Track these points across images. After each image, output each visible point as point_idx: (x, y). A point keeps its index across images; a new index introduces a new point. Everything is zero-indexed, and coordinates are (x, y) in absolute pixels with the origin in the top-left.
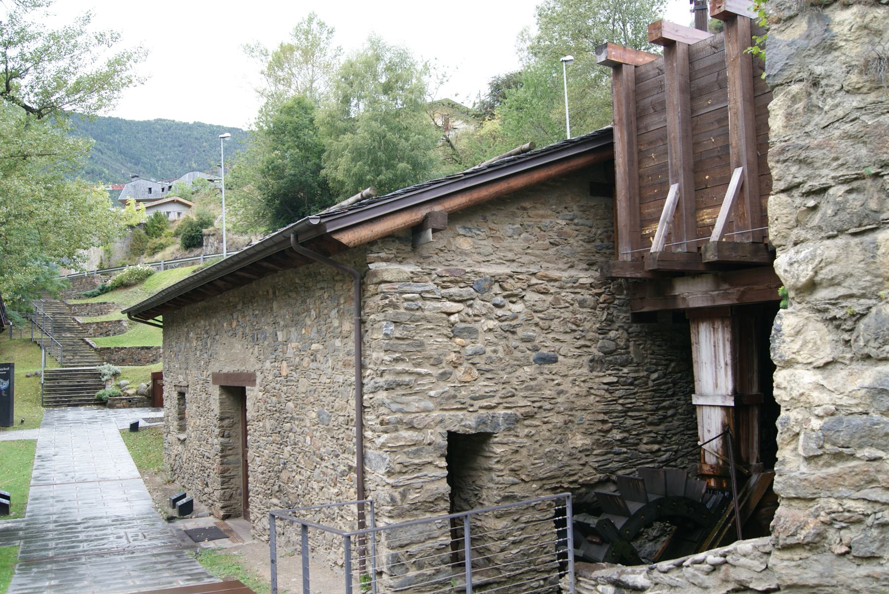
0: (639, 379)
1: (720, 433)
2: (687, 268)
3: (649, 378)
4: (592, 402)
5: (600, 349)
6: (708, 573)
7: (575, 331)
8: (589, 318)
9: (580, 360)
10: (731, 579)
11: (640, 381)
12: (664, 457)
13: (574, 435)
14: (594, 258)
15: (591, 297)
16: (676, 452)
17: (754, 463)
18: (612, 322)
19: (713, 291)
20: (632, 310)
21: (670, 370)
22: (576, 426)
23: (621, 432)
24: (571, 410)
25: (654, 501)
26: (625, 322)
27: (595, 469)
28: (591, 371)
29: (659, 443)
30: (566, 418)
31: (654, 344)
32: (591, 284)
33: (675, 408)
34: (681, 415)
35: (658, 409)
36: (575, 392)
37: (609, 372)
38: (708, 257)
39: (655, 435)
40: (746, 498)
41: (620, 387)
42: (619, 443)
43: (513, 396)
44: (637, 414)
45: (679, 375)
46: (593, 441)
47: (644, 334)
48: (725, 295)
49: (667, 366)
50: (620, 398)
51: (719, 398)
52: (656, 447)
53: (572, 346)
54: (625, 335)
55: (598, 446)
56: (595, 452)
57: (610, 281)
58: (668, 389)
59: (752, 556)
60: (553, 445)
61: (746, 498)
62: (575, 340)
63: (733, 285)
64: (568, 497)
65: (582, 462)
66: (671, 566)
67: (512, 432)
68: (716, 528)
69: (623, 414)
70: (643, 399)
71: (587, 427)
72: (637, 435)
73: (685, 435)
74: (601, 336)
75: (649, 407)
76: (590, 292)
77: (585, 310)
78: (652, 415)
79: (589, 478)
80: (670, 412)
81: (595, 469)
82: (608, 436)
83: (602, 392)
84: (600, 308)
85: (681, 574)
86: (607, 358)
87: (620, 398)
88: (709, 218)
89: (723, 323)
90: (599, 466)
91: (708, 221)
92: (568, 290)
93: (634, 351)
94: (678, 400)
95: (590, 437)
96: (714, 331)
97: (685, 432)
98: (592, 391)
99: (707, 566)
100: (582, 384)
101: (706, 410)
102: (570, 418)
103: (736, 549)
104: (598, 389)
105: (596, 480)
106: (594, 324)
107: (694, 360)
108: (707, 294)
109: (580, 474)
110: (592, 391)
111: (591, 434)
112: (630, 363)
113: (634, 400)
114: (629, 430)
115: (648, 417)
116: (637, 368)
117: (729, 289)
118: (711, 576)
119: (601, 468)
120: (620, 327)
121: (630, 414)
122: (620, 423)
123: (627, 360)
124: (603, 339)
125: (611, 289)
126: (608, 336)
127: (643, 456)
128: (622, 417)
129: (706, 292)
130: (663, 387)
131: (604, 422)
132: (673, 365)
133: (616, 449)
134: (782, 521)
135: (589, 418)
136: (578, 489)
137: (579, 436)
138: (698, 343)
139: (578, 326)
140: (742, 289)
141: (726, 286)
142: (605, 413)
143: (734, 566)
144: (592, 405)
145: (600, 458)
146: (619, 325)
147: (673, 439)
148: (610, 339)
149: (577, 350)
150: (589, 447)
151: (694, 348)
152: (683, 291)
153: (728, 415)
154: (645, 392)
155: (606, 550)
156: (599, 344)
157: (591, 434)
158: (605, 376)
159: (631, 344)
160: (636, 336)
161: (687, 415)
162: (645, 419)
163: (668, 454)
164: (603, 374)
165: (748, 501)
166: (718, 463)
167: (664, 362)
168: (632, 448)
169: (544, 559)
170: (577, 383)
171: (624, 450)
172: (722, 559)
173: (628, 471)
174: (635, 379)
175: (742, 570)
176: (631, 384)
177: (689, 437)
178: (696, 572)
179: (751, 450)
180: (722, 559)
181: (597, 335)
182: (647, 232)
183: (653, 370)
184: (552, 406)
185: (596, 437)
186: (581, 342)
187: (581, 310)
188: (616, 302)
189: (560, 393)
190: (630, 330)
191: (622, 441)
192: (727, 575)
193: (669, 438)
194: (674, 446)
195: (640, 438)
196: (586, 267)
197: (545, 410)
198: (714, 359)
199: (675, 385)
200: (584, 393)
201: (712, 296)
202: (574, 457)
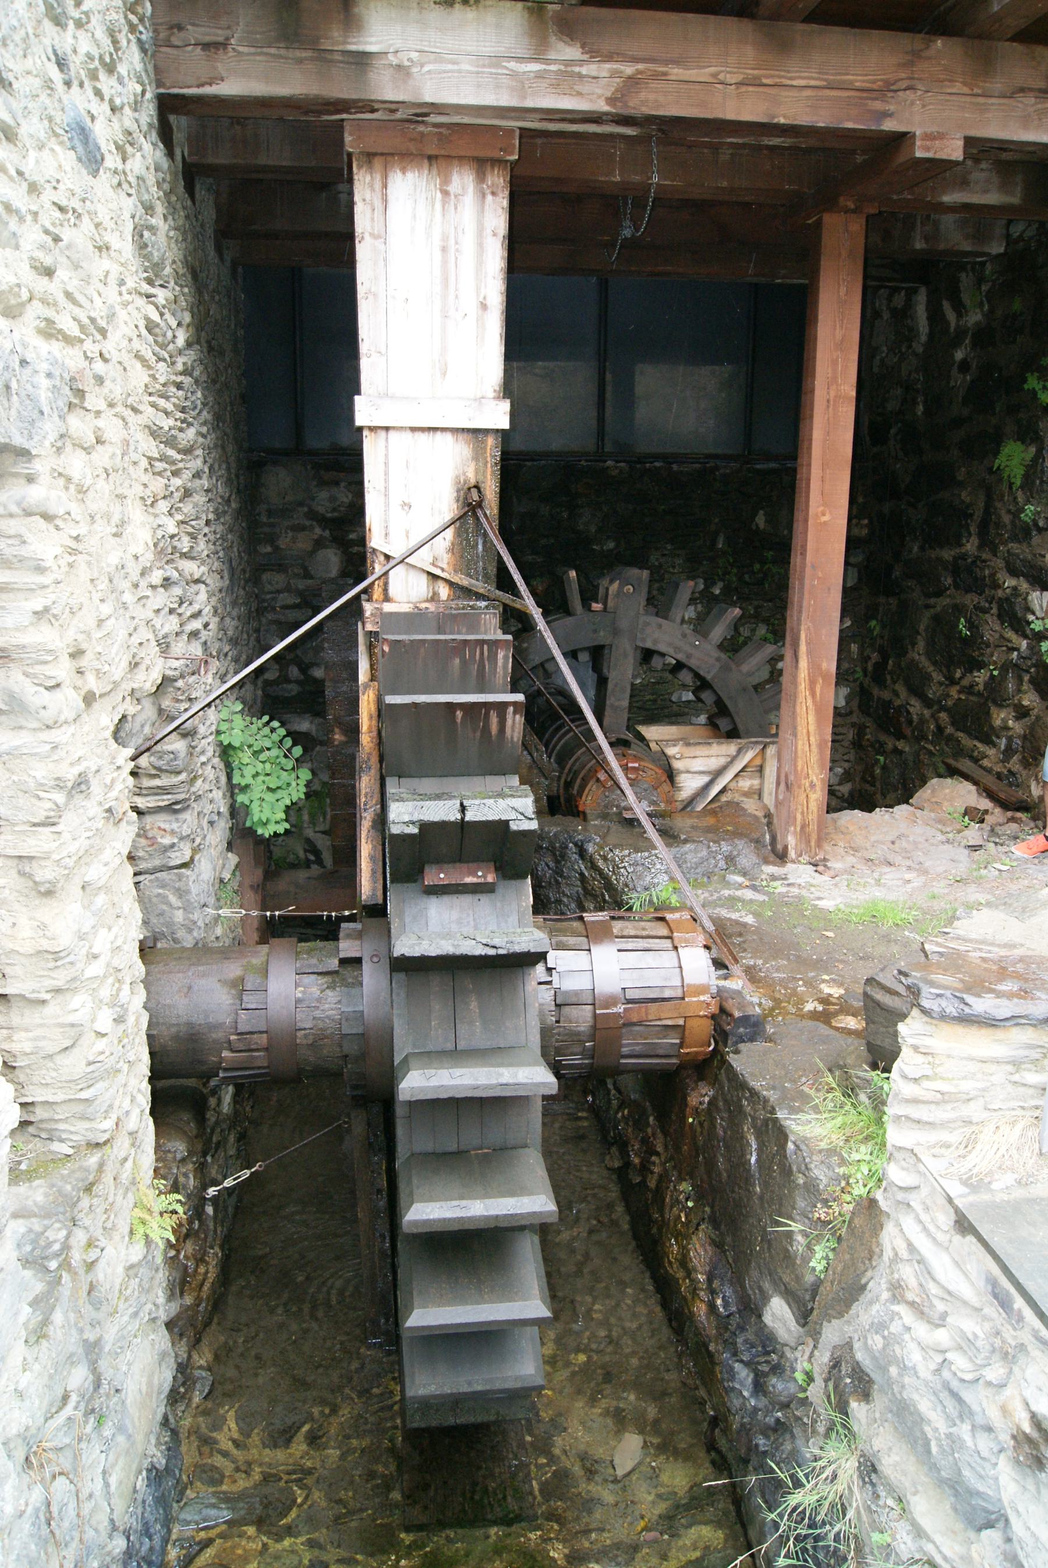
20: (159, 84)
48: (567, 79)
63: (595, 54)
89: (481, 177)
96: (444, 203)
108: (498, 65)
129: (496, 60)
140: (629, 69)
141: (571, 52)
152: (398, 44)
153: (478, 455)
201: (514, 75)
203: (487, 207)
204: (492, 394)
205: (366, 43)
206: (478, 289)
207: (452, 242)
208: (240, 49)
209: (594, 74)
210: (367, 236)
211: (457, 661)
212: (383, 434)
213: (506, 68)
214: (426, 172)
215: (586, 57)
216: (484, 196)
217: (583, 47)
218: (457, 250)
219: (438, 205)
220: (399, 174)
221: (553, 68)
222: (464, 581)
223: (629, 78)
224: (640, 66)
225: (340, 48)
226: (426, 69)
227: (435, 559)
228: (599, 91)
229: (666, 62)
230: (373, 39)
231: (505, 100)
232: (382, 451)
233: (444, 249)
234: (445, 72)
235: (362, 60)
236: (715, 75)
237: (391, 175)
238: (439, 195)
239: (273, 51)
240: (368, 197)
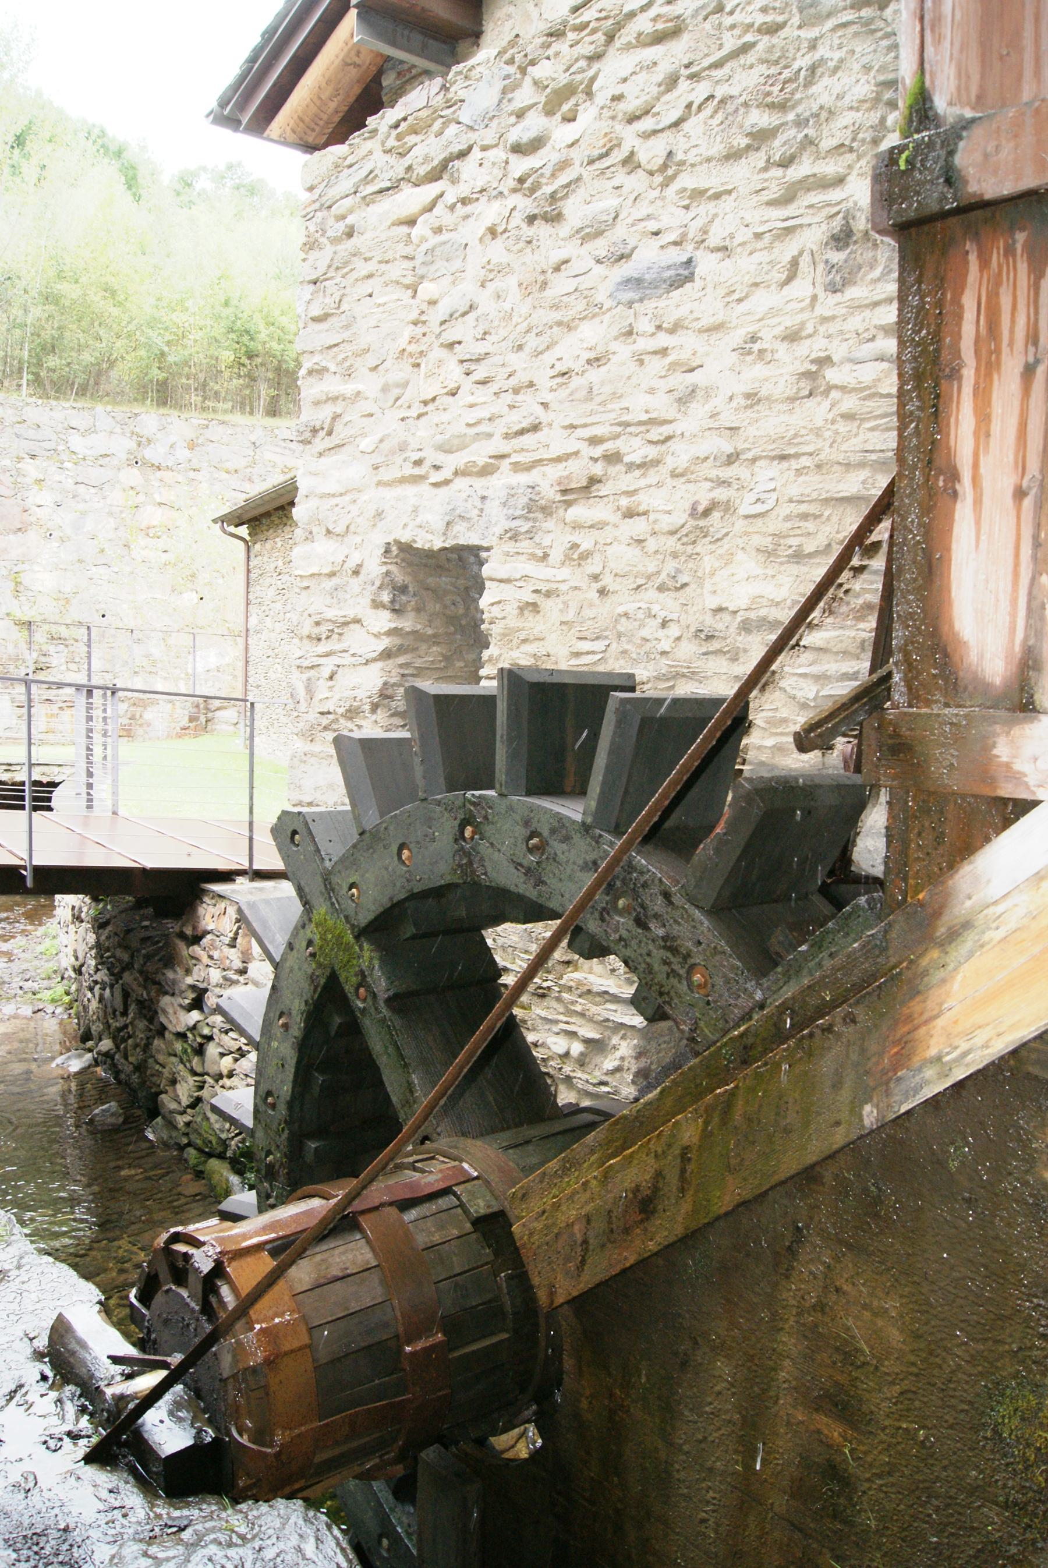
13: (728, 559)
22: (740, 525)
24: (732, 459)
30: (704, 495)
43: (535, 428)
60: (652, 594)
67: (524, 545)
95: (794, 569)
102: (721, 494)
137: (747, 564)
144: (818, 432)
169: (592, 978)
184: (652, 452)
189: (685, 399)
197: (631, 467)
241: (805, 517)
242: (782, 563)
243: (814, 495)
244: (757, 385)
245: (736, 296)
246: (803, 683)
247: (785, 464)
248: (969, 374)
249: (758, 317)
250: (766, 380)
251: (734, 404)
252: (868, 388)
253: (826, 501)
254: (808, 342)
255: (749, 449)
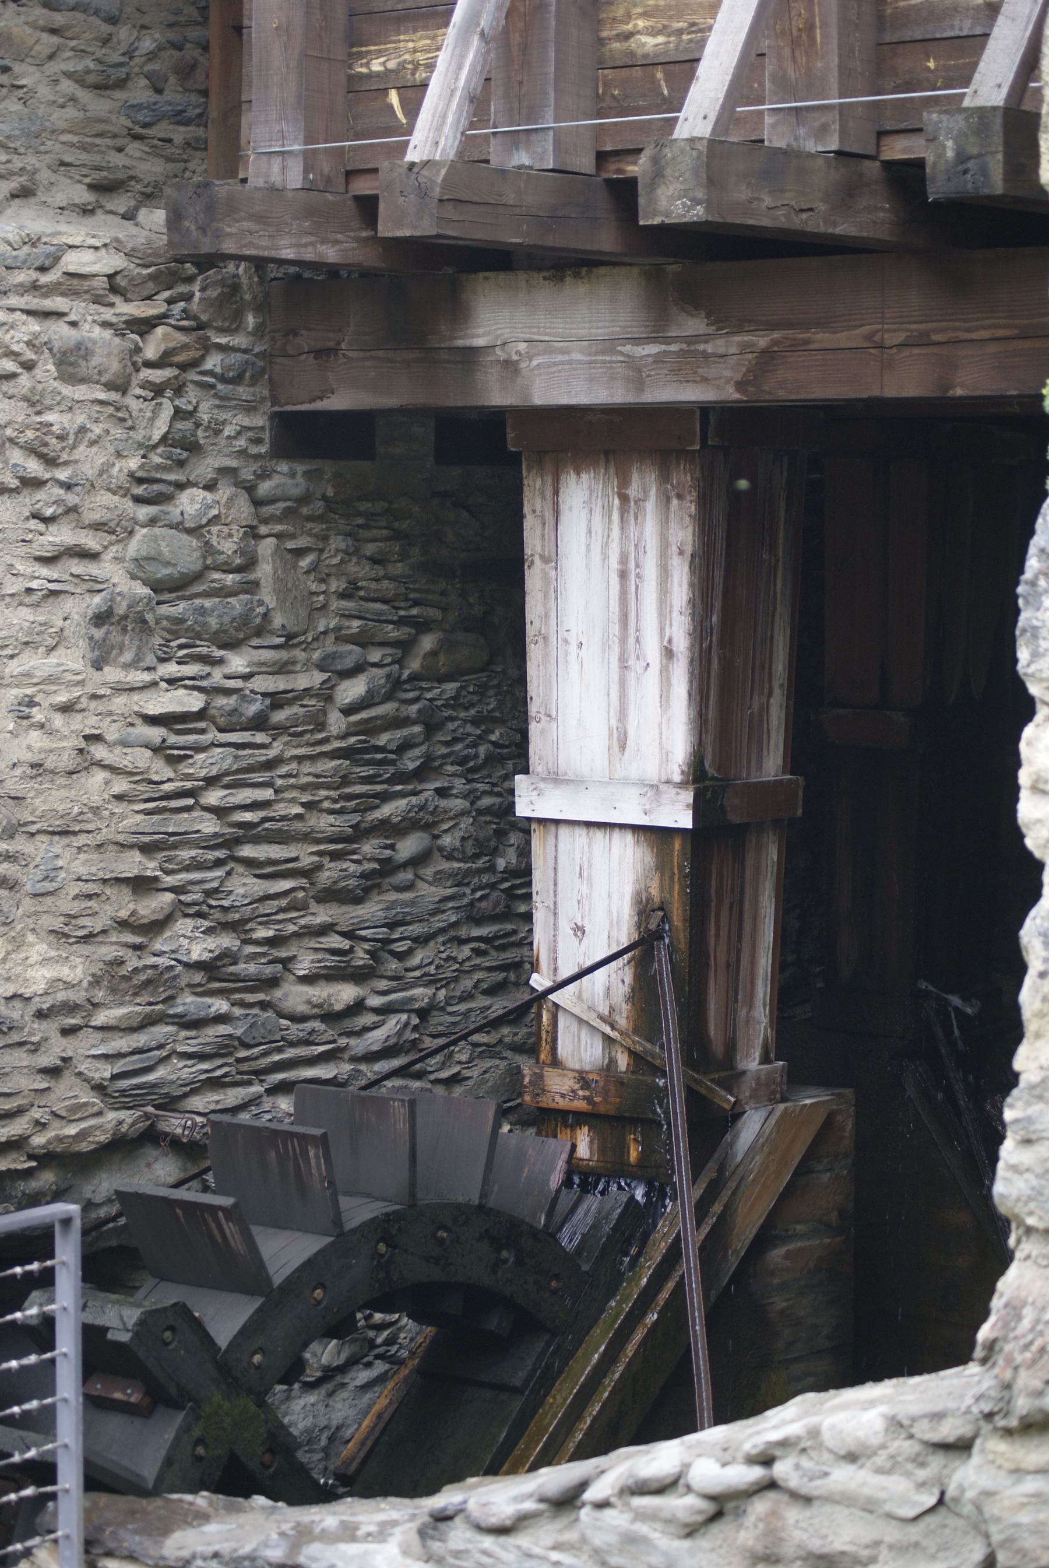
0: (290, 702)
1: (625, 943)
2: (551, 241)
3: (329, 699)
4: (96, 800)
5: (138, 569)
6: (691, 1531)
7: (37, 483)
8: (97, 430)
9: (53, 614)
10: (788, 1550)
11: (296, 709)
12: (376, 1039)
14: (118, 160)
15: (108, 334)
16: (423, 1014)
17: (751, 1063)
18: (193, 448)
19: (636, 341)
21: (415, 664)
22: (28, 904)
23: (208, 931)
25: (363, 1225)
26: (243, 453)
27: (99, 1088)
28: (98, 665)
29: (359, 976)
31: (356, 552)
32: (111, 277)
33: (427, 827)
34: (449, 857)
35: (359, 833)
36: (29, 757)
37: (171, 669)
38: (663, 203)
39: (345, 944)
40: (717, 1208)
41: (213, 735)
42: (198, 977)
44: (276, 852)
45: (450, 688)
46: (96, 969)
47: (319, 507)
49: (405, 646)
50: (211, 782)
51: (635, 791)
52: (345, 994)
53: (23, 550)
54: (243, 510)
55: (113, 990)
56: (101, 1018)
57: (190, 269)
58: (405, 747)
59: (881, 1459)
61: (717, 1208)
62: (33, 524)
64: (66, 1222)
65: (46, 1060)
66: (530, 1506)
68: (597, 1331)
69: (220, 854)
70: (303, 788)
71: (75, 907)
72: (272, 942)
73: (462, 942)
74: (144, 512)
75: (324, 823)
76: (107, 314)
77: (81, 392)
78: (335, 856)
79: (72, 1130)
80: (408, 846)
81: (99, 1088)
82: (158, 946)
83: (142, 758)
84: (146, 385)
85: (571, 1536)
86: (164, 610)
87: (211, 782)
88: (652, 32)
89: (664, 477)
90: (115, 1077)
91: (650, 43)
92: (14, 301)
93: (277, 580)
94: (442, 793)
96: (623, 511)
97: (463, 932)
98: (99, 752)
99: (690, 1500)
100: (58, 721)
101: (572, 842)
103: (814, 1433)
104: (124, 743)
105: (102, 1138)
106: (119, 454)
107: (530, 631)
108: (612, 351)
109: (36, 1114)
110: (99, 752)
111: (88, 938)
112: (259, 632)
113: (267, 794)
114: (244, 921)
115: (319, 867)
116: (283, 655)
117: (706, 338)
118: (703, 1542)
119: (125, 1084)
120: (224, 471)
121: (247, 851)
122: (209, 893)
123: (244, 620)
124: (153, 522)
125: (195, 306)
126: (174, 511)
127: (296, 1031)
128: (218, 863)
129: (610, 344)
130: (383, 739)
131: (141, 885)
132: (428, 642)
133: (188, 1003)
134: (1026, 1323)
135: (83, 871)
136: (28, 1173)
137: (38, 949)
138: (552, 558)
139: (51, 462)
140: (762, 341)
141: (694, 325)
142: (147, 849)
143: (807, 1500)
144: (96, 810)
145: (122, 1043)
146: (218, 463)
147: (416, 961)
148: (178, 526)
149: (44, 571)
150: (77, 996)
151: (533, 579)
152: (506, 334)
153: (662, 865)
154: (312, 758)
155: (169, 1436)
156: (135, 546)
157: (88, 938)
158: (154, 684)
159: (266, 547)
160: (288, 514)
161: (476, 857)
162: (307, 873)
163: (393, 1023)
164: (147, 677)
165: (724, 1220)
166: (612, 1062)
167: (392, 632)
168: (250, 998)
170: (38, 715)
171: (220, 1005)
172: (757, 1473)
173: (232, 1097)
174: (276, 700)
175: (840, 1513)
176: (259, 723)
177: (478, 952)
178: (643, 1529)
179: (743, 1013)
180: (757, 1473)
181: (128, 504)
182: (376, 66)
183: (348, 663)
185: (108, 951)
186: (62, 535)
187: (67, 390)
188: (213, 362)
190: (265, 488)
191: (209, 967)
192: (772, 1532)
193: (401, 956)
194: (418, 991)
195: (283, 954)
196: (82, 195)
198: (615, 629)
199: (431, 728)
200: (66, 760)
201: (630, 362)
202: (15, 1037)
203: (672, 515)
204: (677, 778)
205: (473, 336)
206: (662, 630)
207: (632, 565)
208: (350, 354)
209: (721, 351)
210: (537, 559)
211: (273, 1154)
212: (553, 828)
213: (621, 353)
214: (602, 470)
215: (711, 330)
216: (668, 500)
217: (708, 317)
218: (638, 576)
219: (616, 516)
220: (573, 476)
221: (674, 348)
222: (640, 1045)
223: (764, 352)
224: (776, 335)
225: (447, 344)
226: (535, 363)
227: (612, 1009)
228: (727, 374)
229: (805, 326)
230: (480, 331)
231: (617, 394)
232: (550, 849)
233: (623, 575)
234: (555, 364)
235: (470, 356)
236: (869, 337)
237: (563, 477)
238: (617, 501)
239: (381, 354)
240: (538, 508)
241: (89, 897)
242: (71, 944)
243: (101, 874)
244: (43, 756)
245: (8, 652)
246: (99, 1064)
247: (65, 840)
248: (713, 904)
249: (35, 680)
250: (51, 751)
251: (18, 772)
252: (142, 773)
253: (105, 881)
254: (79, 717)
255: (33, 823)
